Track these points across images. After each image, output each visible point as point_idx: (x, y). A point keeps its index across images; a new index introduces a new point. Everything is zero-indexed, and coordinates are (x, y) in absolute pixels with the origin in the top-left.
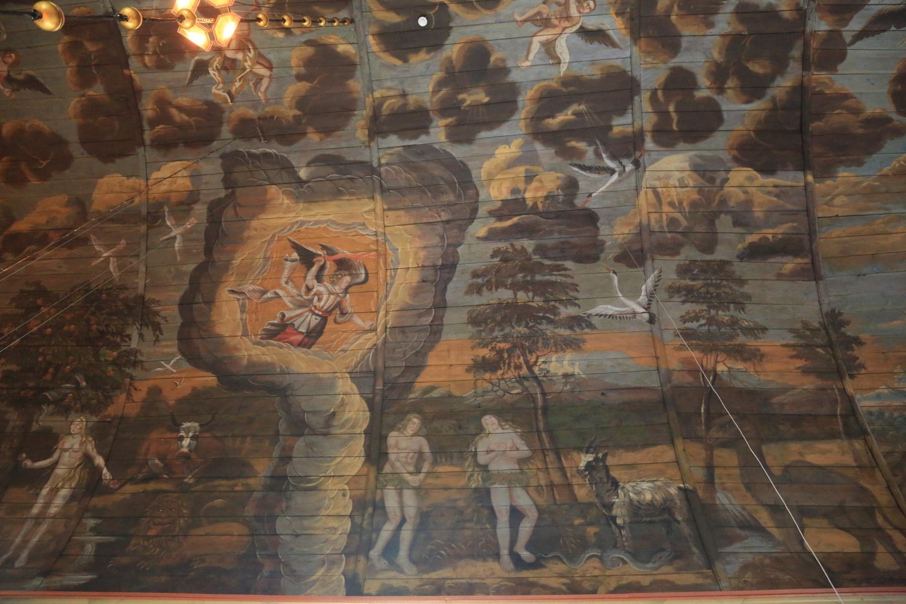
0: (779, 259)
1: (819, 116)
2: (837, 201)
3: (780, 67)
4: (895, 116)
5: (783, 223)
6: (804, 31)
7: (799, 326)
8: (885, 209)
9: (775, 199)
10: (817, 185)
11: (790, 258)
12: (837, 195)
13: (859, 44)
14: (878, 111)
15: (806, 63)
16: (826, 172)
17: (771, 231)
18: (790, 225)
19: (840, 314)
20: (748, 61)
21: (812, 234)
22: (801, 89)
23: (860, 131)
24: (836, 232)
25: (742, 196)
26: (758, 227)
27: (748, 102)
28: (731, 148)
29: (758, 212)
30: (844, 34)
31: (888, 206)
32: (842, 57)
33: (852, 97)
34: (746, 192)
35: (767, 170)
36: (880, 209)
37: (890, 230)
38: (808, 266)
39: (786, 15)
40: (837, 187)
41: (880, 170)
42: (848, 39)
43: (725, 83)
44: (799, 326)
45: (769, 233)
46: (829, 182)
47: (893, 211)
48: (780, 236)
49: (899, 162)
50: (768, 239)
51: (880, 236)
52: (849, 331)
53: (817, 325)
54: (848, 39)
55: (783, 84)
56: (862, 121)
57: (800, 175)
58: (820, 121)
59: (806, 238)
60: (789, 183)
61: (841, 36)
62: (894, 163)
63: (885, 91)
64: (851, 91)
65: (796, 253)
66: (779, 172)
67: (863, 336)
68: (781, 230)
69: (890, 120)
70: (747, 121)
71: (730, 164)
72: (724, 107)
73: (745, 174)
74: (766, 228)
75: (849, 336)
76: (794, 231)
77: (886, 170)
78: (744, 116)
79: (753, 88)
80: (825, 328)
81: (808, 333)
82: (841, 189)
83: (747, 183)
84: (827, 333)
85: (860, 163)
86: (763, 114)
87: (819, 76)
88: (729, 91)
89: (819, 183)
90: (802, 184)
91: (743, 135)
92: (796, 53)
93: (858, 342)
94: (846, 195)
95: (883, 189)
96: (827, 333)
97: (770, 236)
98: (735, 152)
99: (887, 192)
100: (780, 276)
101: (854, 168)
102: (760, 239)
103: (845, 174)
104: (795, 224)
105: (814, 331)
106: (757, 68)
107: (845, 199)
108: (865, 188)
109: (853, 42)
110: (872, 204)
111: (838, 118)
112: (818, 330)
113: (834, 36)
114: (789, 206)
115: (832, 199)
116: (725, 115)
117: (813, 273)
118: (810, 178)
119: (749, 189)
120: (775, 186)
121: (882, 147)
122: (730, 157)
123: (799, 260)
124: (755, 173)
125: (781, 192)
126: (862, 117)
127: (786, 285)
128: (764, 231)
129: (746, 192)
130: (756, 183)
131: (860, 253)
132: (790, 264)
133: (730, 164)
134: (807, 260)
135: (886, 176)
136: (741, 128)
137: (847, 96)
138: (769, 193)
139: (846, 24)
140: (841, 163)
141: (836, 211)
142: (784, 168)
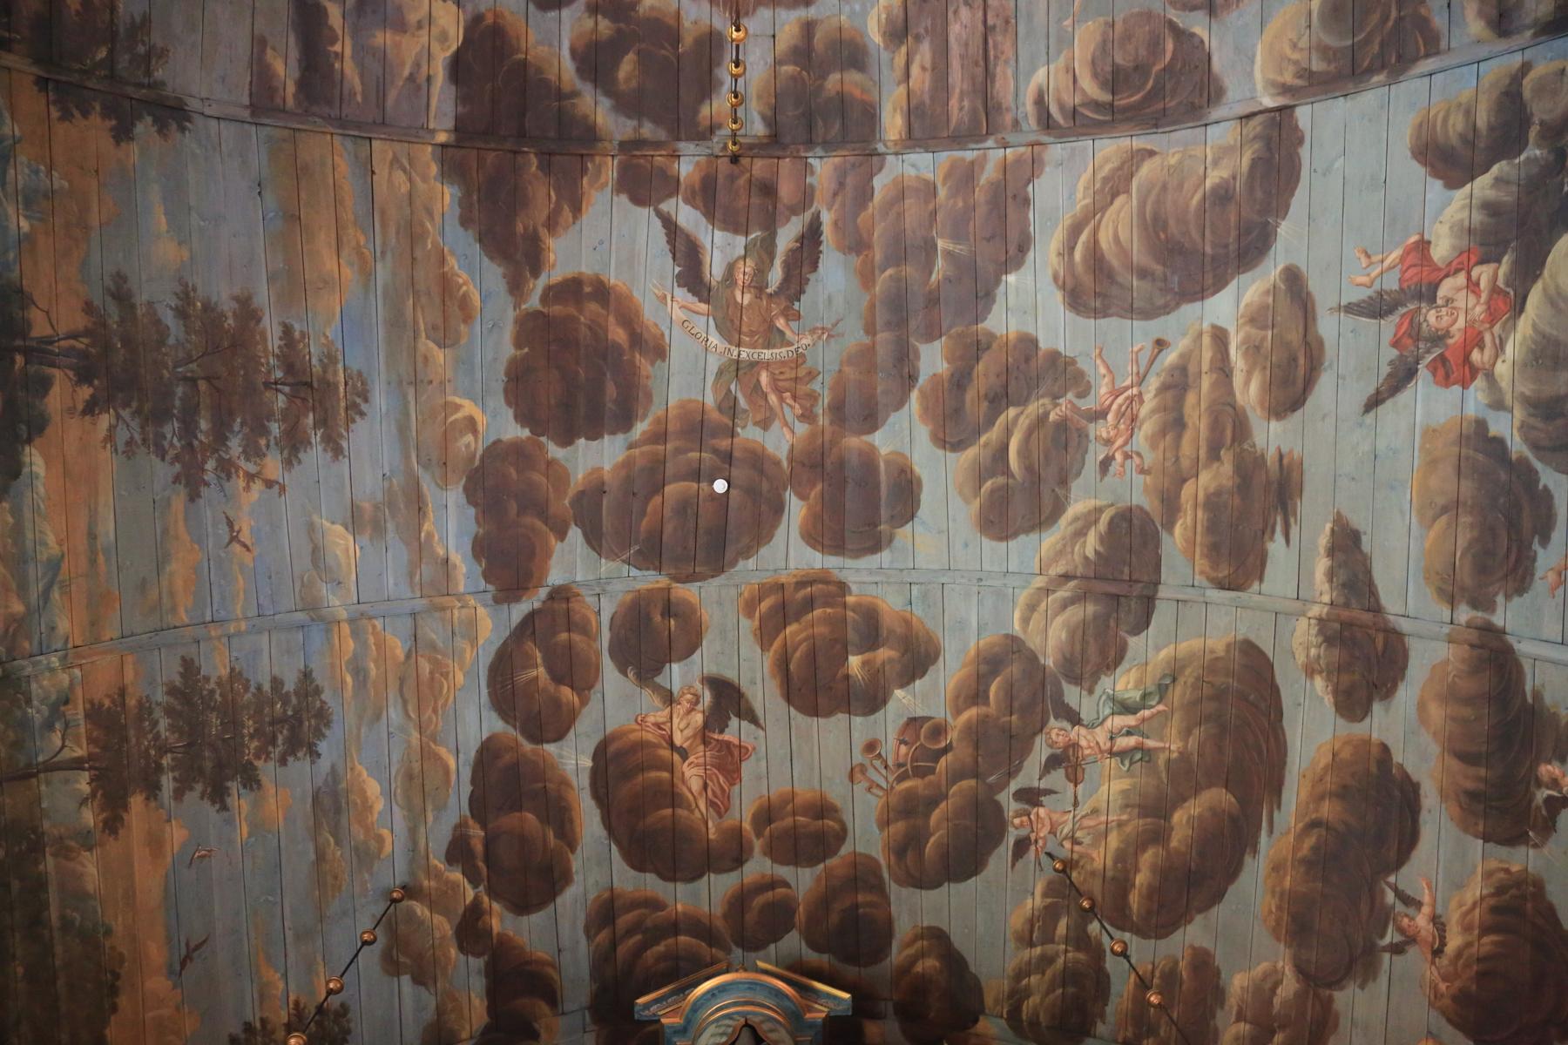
0: (294, 53)
1: (546, 167)
2: (400, 177)
3: (628, 105)
4: (541, 283)
5: (362, 76)
6: (679, 140)
7: (157, 39)
8: (383, 253)
9: (406, 73)
10: (430, 149)
11: (297, 75)
12: (410, 180)
13: (657, 223)
14: (552, 257)
15: (630, 146)
16: (452, 163)
17: (348, 52)
18: (359, 88)
19: (182, 129)
20: (638, 53)
21: (342, 123)
22: (589, 136)
23: (520, 228)
24: (344, 165)
25: (412, 18)
26: (356, 32)
27: (573, 52)
28: (496, 15)
29: (382, 38)
30: (673, 201)
31: (389, 255)
32: (638, 200)
33: (575, 218)
34: (419, 26)
35: (457, 68)
36: (384, 244)
37: (345, 253)
38: (278, 101)
39: (705, 111)
40: (425, 179)
41: (452, 253)
42: (664, 207)
43: (605, 16)
44: (157, 39)
45: (344, 47)
46: (434, 169)
47: (379, 266)
48: (337, 66)
49: (465, 283)
50: (333, 43)
51: (334, 236)
52: (144, 127)
53: (159, 74)
54: (664, 207)
55: (599, 111)
56: (535, 230)
57: (450, 124)
58: (540, 167)
59: (335, 113)
60: (434, 102)
61: (670, 196)
62: (465, 276)
63: (584, 269)
64: (585, 218)
65: (303, 85)
66: (453, 88)
67: (134, 149)
68: (350, 68)
69: (536, 273)
70: (542, 50)
71: (469, 7)
72: (565, 13)
73: (452, 32)
74: (354, 47)
75: (133, 125)
76: (346, 92)
77: (452, 262)
78: (550, 45)
79: (595, 61)
80: (149, 86)
81: (141, 49)
82: (421, 185)
83: (435, 31)
84: (140, 85)
85: (465, 222)
86: (553, 78)
87: (610, 169)
88: (589, 23)
89: (433, 153)
90: (431, 126)
91: (518, 38)
92: (648, 130)
93: (123, 133)
94: (410, 194)
95: (418, 254)
96: (140, 85)
97: (337, 48)
98: (489, 20)
99: (414, 259)
100: (260, 44)
101: (457, 211)
102: (331, 29)
103: (447, 197)
104: (359, 98)
105: (147, 61)
106: (627, 67)
107: (405, 188)
108: (422, 225)
109: (659, 214)
110: (392, 230)
111: (542, 194)
112: (148, 73)
113: (672, 186)
114: (392, 95)
115: (404, 171)
116: (553, 14)
117: (263, 102)
118: (442, 138)
119: (425, 32)
120: (429, 79)
121: (491, 258)
122: (483, 9)
123: (291, 89)
124: (454, 48)
125: (418, 85)
126: (543, 232)
127: (243, 47)
128: (348, 42)
129: (419, 26)
130: (436, 48)
131: (303, 195)
132: (285, 68)
133: (469, 7)
134: (290, 102)
135: (443, 261)
136: (532, 39)
137: (577, 210)
138: (417, 65)
139: (686, 201)
140: (467, 194)
141: (382, 171)
142: (462, 99)
